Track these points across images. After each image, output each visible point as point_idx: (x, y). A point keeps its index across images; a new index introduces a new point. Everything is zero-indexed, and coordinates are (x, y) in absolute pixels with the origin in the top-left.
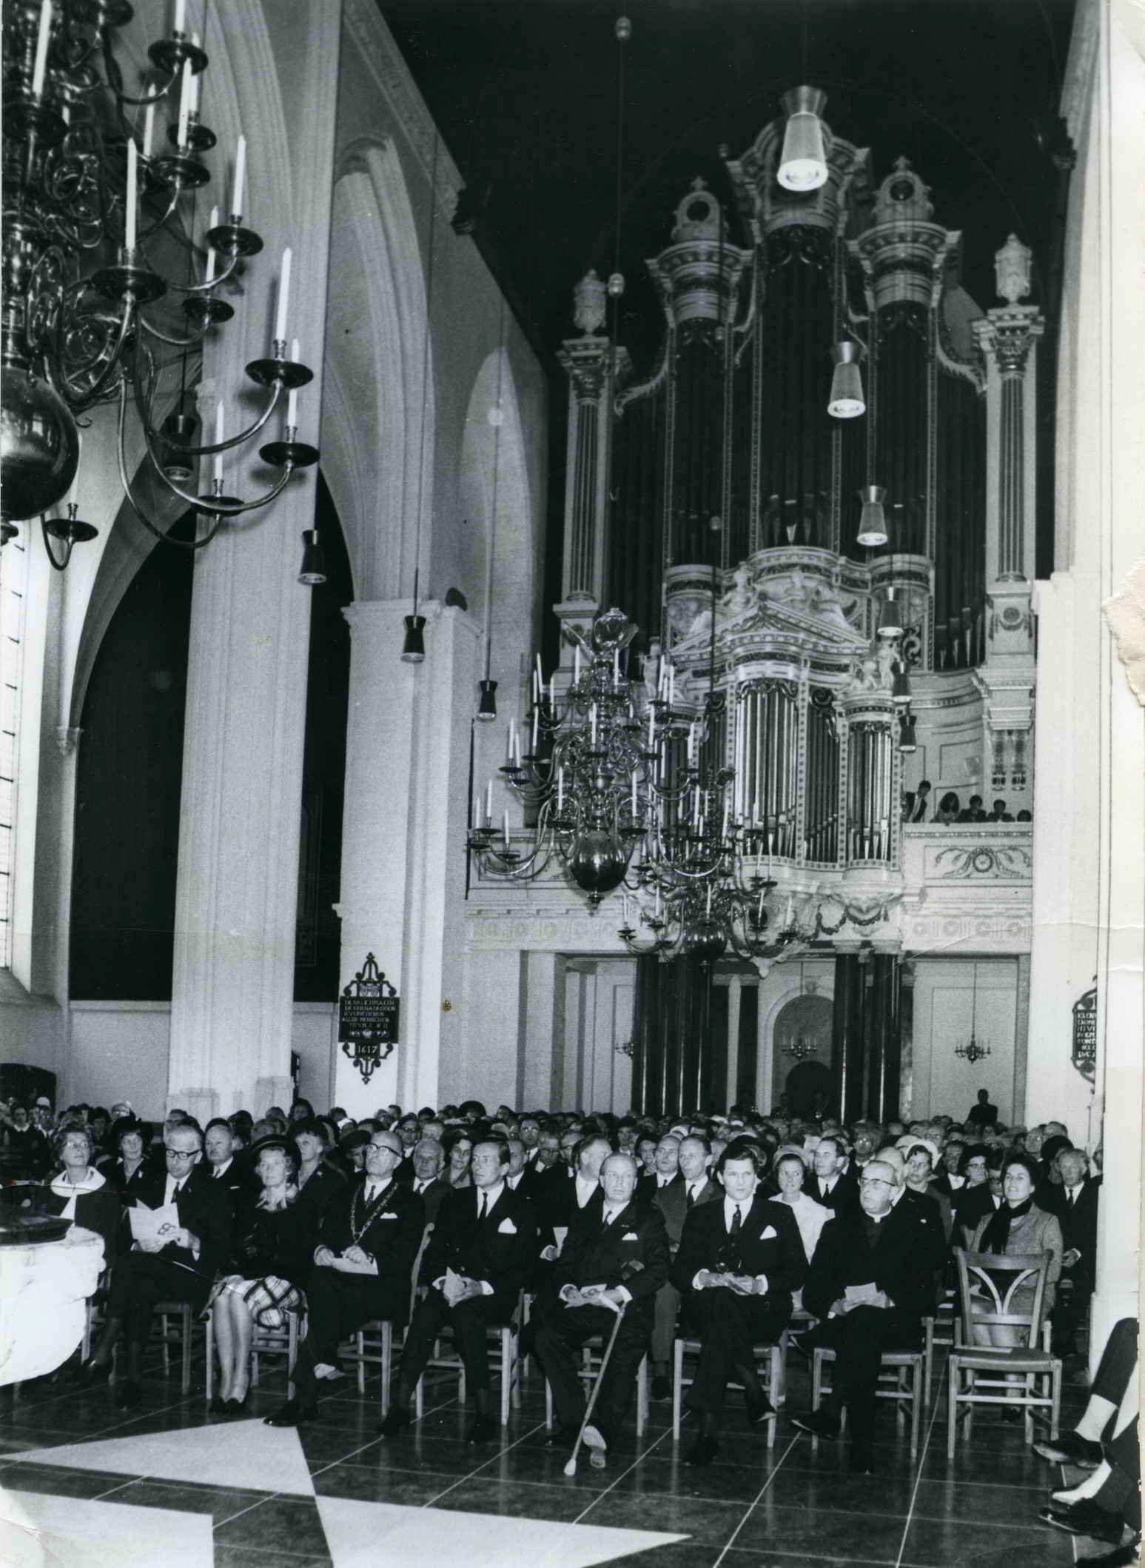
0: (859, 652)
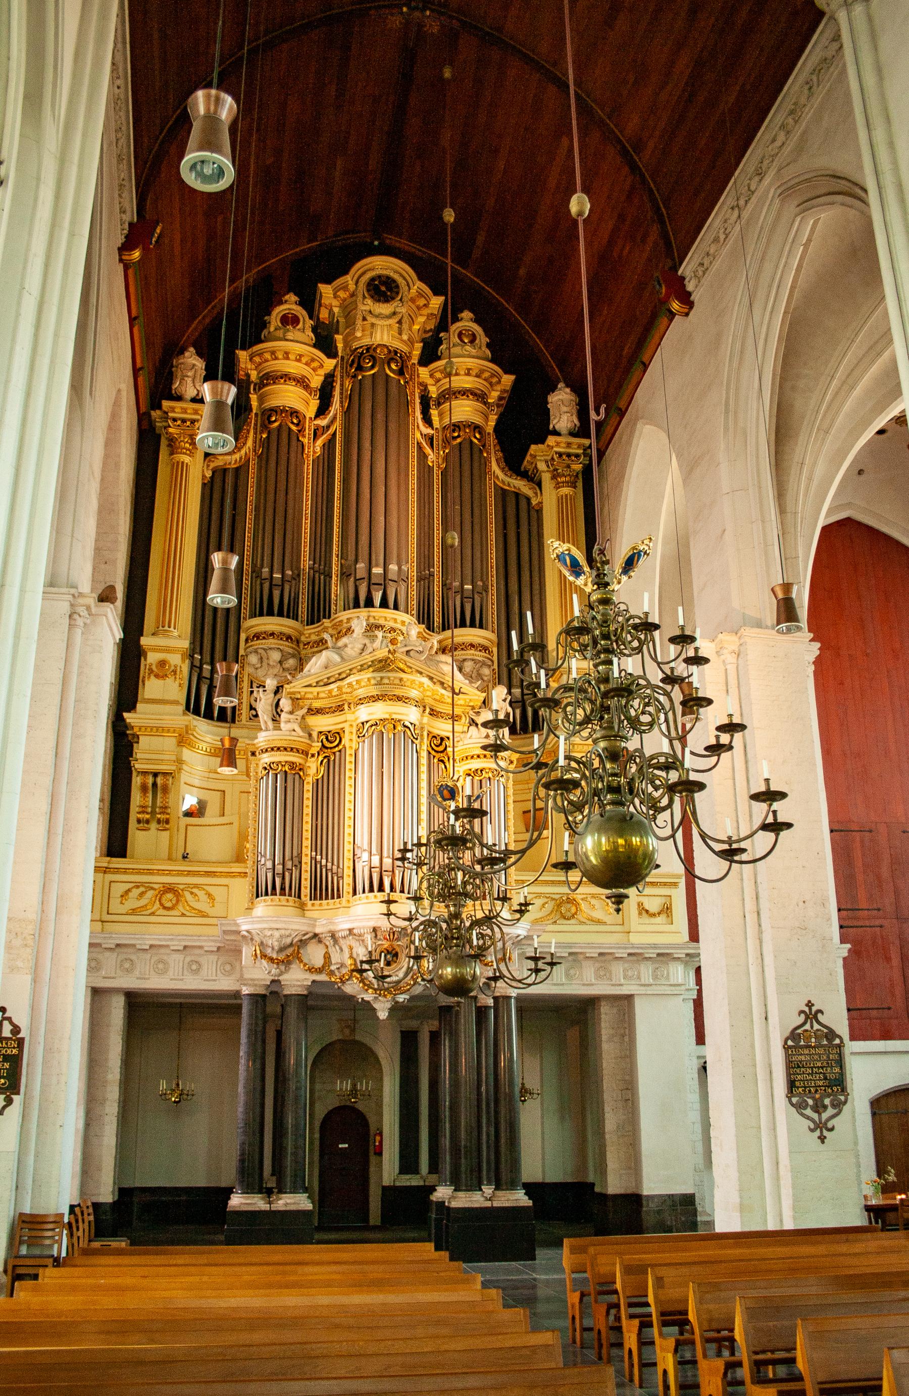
0: (472, 704)
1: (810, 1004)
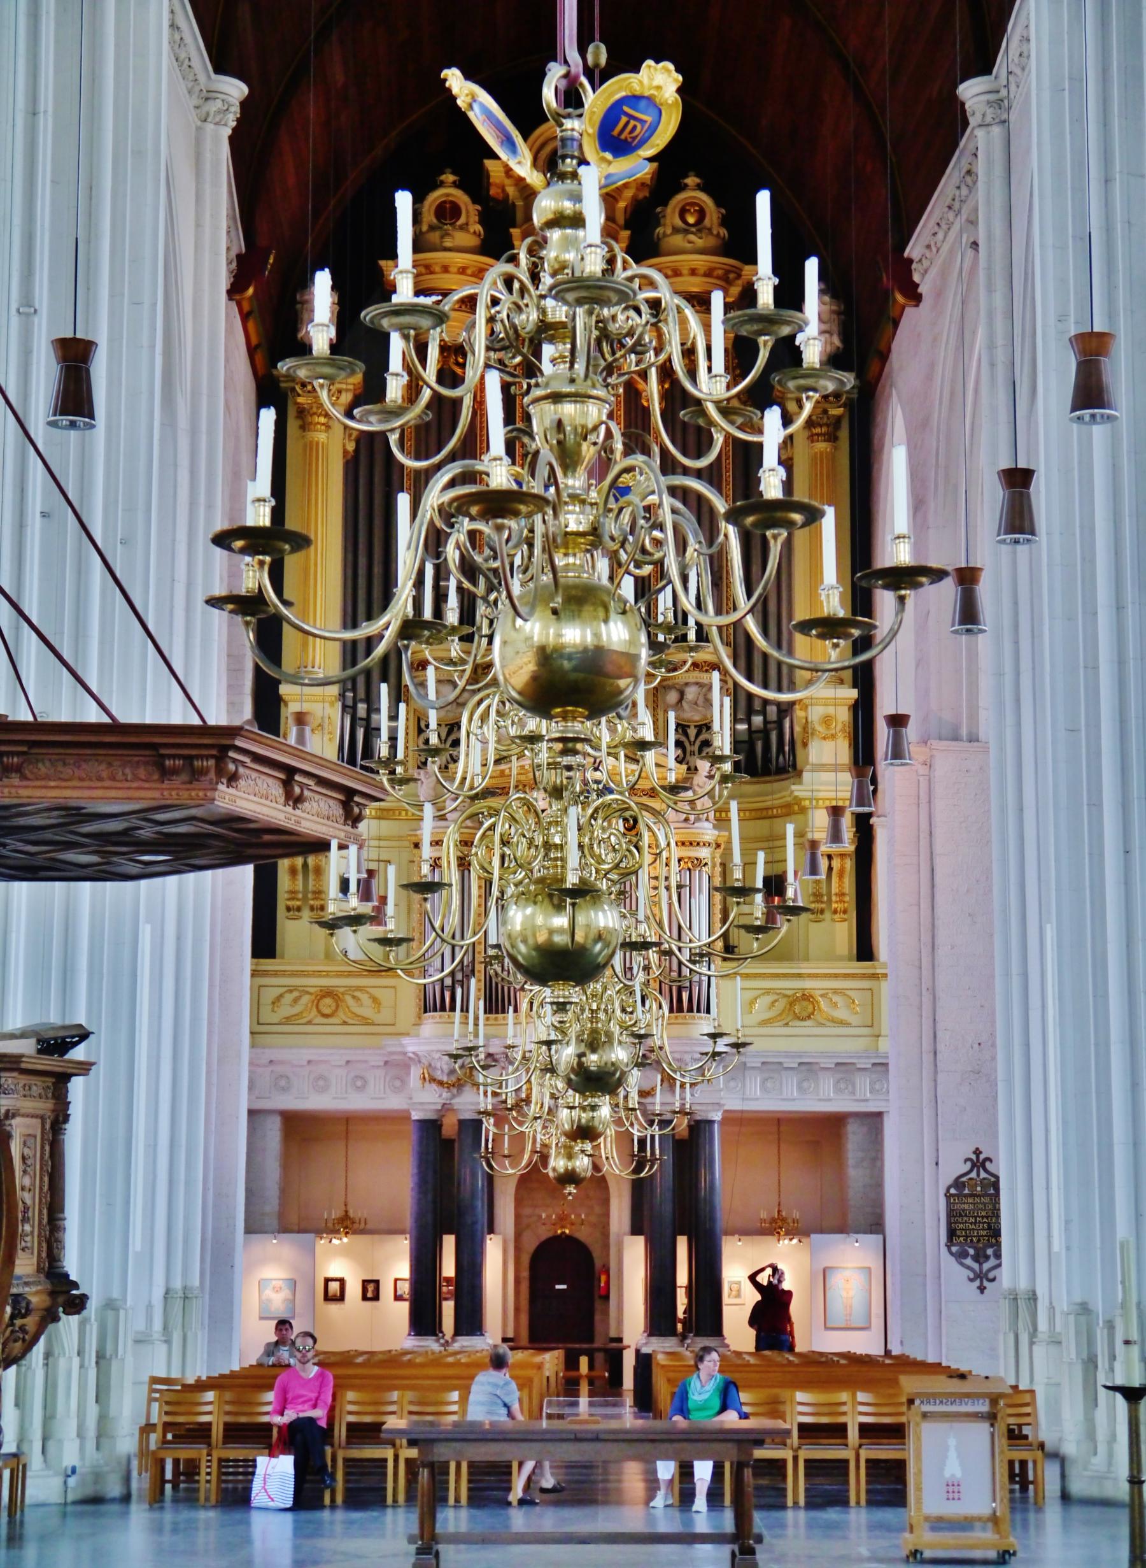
1: (977, 1152)
